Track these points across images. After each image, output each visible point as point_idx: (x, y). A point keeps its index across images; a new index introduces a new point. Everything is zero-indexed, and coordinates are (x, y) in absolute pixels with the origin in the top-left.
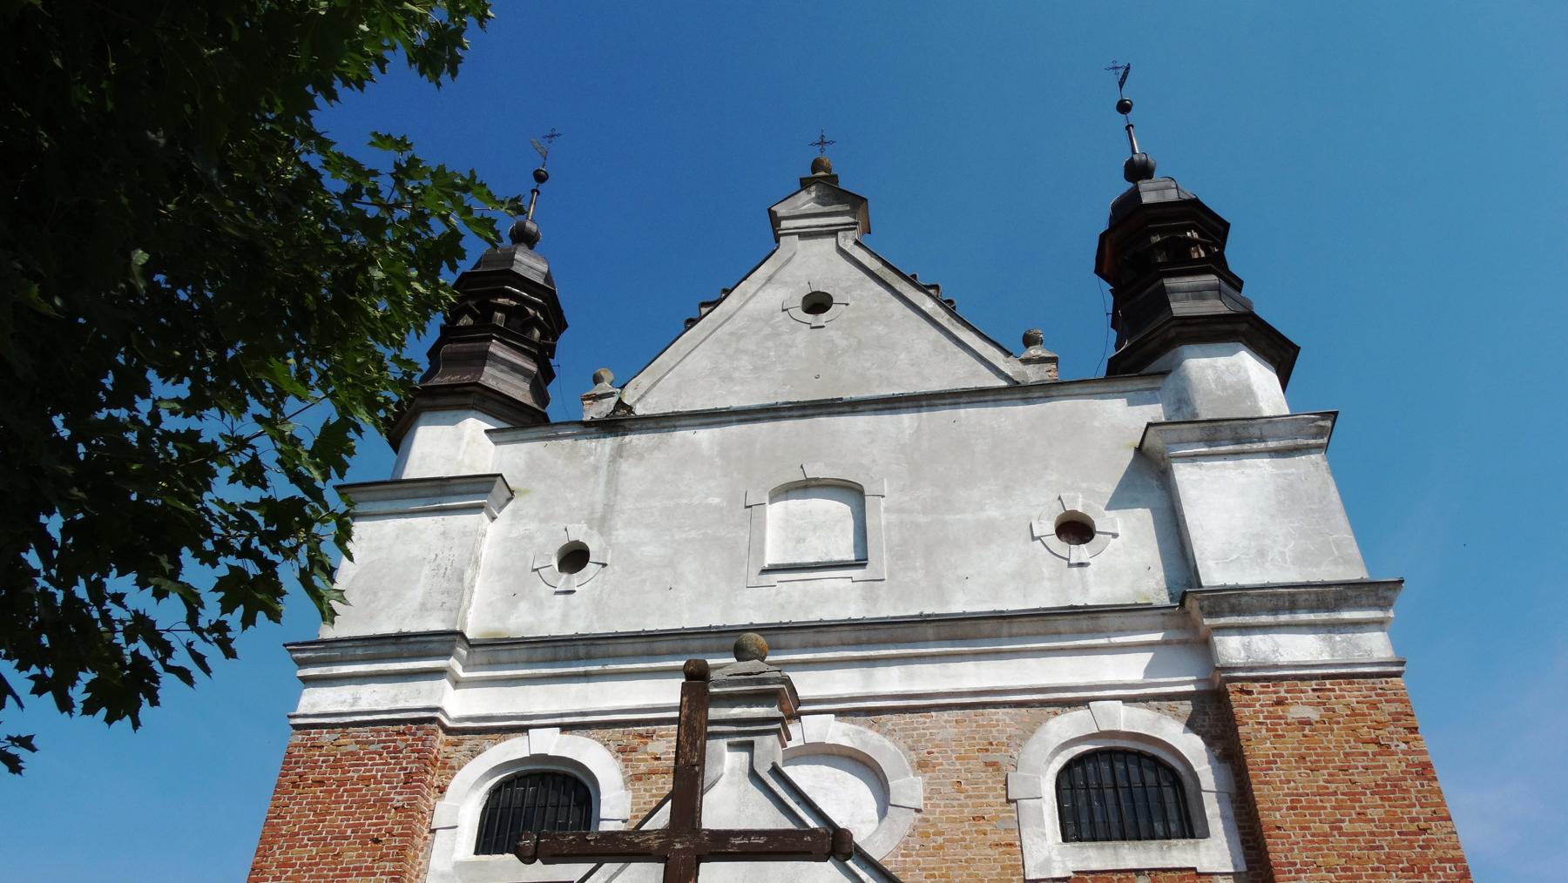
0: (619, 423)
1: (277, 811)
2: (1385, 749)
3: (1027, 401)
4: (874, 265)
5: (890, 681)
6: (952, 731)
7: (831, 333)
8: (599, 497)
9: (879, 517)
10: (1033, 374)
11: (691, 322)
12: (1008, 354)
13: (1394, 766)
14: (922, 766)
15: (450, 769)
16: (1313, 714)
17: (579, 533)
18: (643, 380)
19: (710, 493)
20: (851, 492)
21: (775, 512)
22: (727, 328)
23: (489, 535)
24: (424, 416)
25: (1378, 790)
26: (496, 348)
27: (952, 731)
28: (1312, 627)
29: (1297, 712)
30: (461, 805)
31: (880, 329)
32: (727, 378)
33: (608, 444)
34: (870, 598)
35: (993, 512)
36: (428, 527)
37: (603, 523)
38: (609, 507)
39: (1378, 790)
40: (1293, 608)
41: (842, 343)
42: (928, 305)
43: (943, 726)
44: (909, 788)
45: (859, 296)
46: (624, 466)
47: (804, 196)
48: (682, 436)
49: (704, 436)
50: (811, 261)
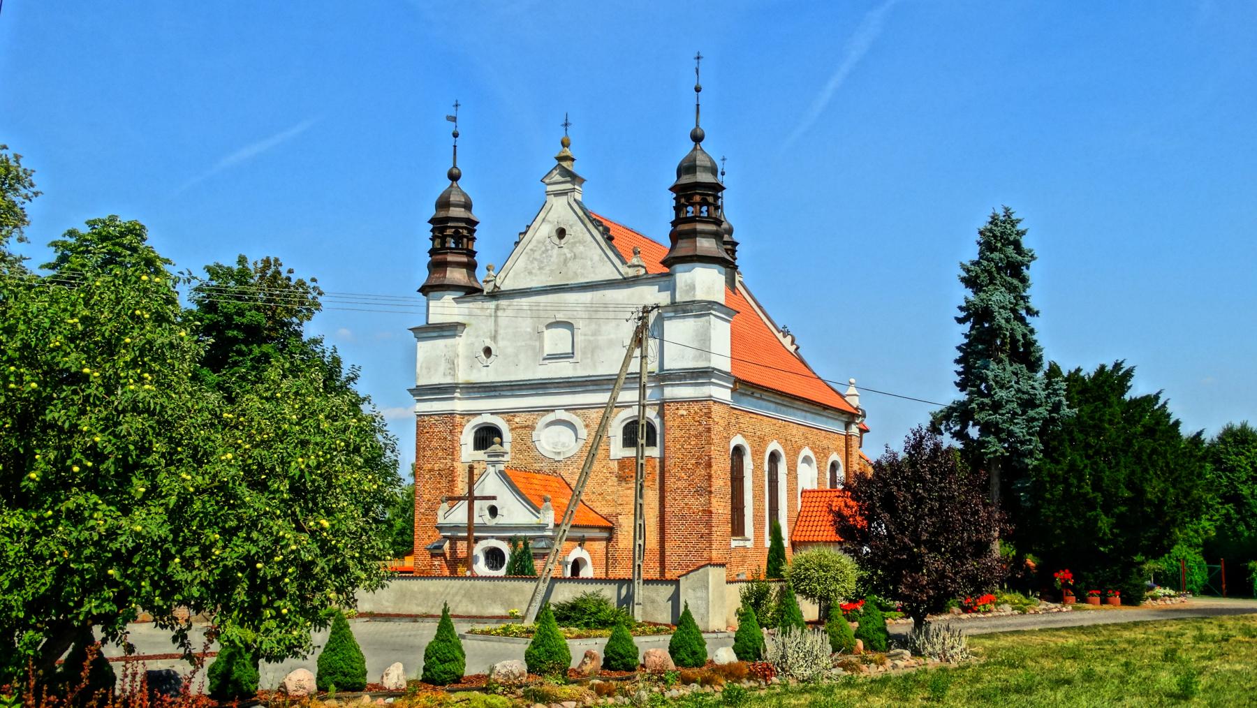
0: (495, 295)
1: (418, 441)
2: (700, 424)
3: (629, 286)
4: (581, 213)
6: (595, 415)
7: (565, 250)
8: (493, 328)
9: (579, 338)
10: (631, 272)
11: (517, 243)
12: (624, 262)
13: (701, 429)
14: (587, 426)
15: (462, 426)
16: (685, 413)
17: (489, 343)
18: (502, 274)
19: (526, 325)
20: (568, 325)
21: (549, 334)
22: (530, 247)
23: (460, 343)
24: (431, 294)
25: (696, 436)
26: (450, 258)
27: (595, 415)
28: (692, 385)
30: (467, 437)
31: (581, 248)
32: (530, 273)
33: (492, 305)
34: (575, 369)
35: (612, 336)
36: (441, 343)
38: (496, 331)
39: (696, 436)
40: (685, 378)
41: (569, 256)
42: (599, 237)
44: (583, 433)
45: (577, 230)
46: (500, 313)
47: (555, 172)
48: (516, 301)
49: (524, 302)
50: (560, 210)
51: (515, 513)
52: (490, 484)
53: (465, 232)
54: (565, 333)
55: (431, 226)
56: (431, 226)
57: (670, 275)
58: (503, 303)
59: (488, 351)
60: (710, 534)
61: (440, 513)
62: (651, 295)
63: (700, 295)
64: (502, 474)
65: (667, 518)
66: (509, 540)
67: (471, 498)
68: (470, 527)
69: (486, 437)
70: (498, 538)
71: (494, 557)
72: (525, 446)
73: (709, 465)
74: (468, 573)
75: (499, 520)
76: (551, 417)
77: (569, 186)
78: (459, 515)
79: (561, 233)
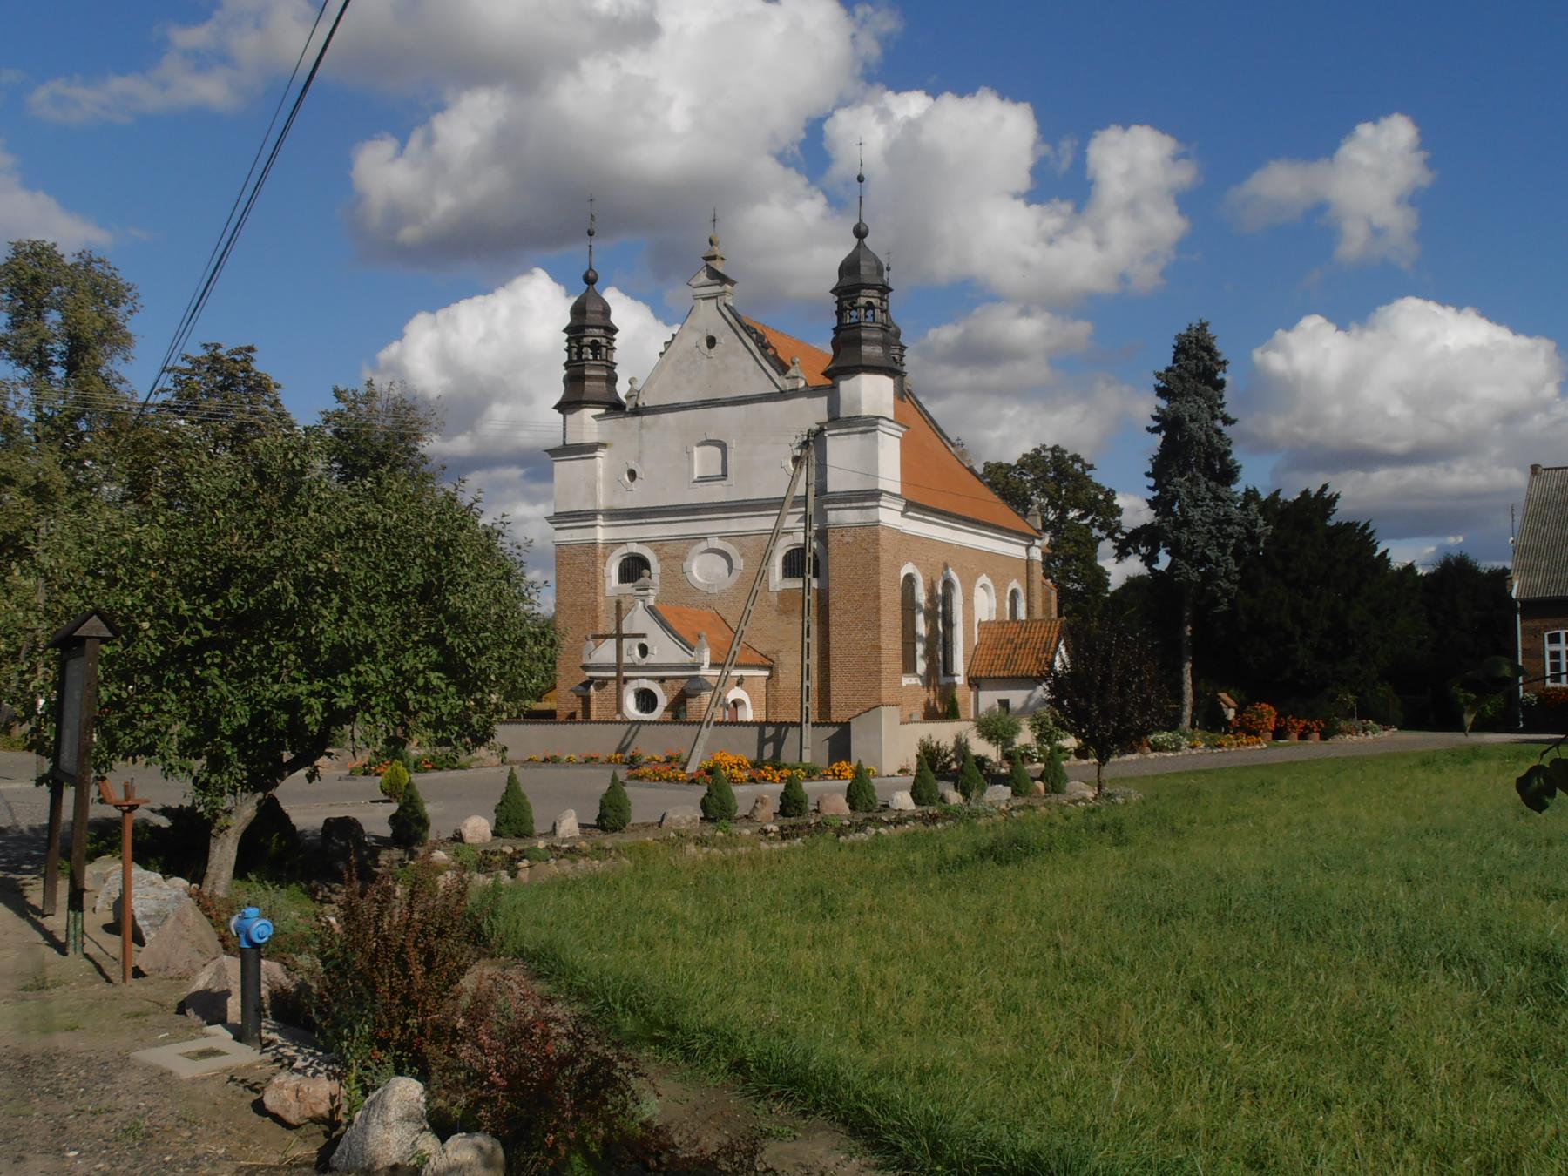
0: (637, 411)
5: (736, 525)
9: (731, 459)
14: (743, 555)
15: (606, 556)
20: (723, 446)
21: (697, 451)
29: (848, 539)
30: (613, 570)
33: (637, 419)
37: (639, 460)
42: (752, 346)
43: (748, 541)
44: (739, 563)
45: (726, 337)
46: (644, 432)
51: (665, 650)
52: (638, 620)
53: (604, 341)
54: (717, 451)
55: (566, 336)
56: (566, 336)
57: (835, 387)
58: (647, 418)
59: (632, 474)
60: (879, 671)
61: (585, 652)
62: (813, 411)
63: (866, 410)
64: (652, 611)
65: (832, 653)
66: (662, 680)
67: (620, 637)
68: (618, 666)
69: (633, 568)
70: (649, 678)
71: (646, 700)
72: (676, 577)
73: (878, 597)
74: (618, 717)
75: (651, 659)
76: (703, 546)
77: (717, 289)
78: (605, 653)
79: (711, 342)
